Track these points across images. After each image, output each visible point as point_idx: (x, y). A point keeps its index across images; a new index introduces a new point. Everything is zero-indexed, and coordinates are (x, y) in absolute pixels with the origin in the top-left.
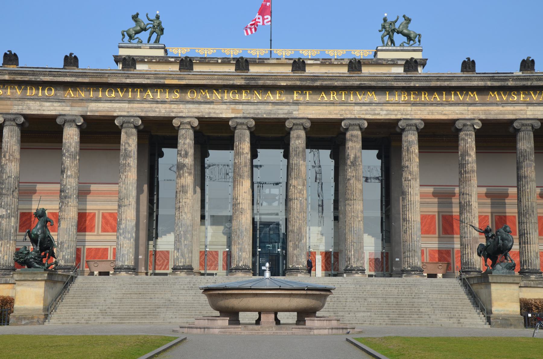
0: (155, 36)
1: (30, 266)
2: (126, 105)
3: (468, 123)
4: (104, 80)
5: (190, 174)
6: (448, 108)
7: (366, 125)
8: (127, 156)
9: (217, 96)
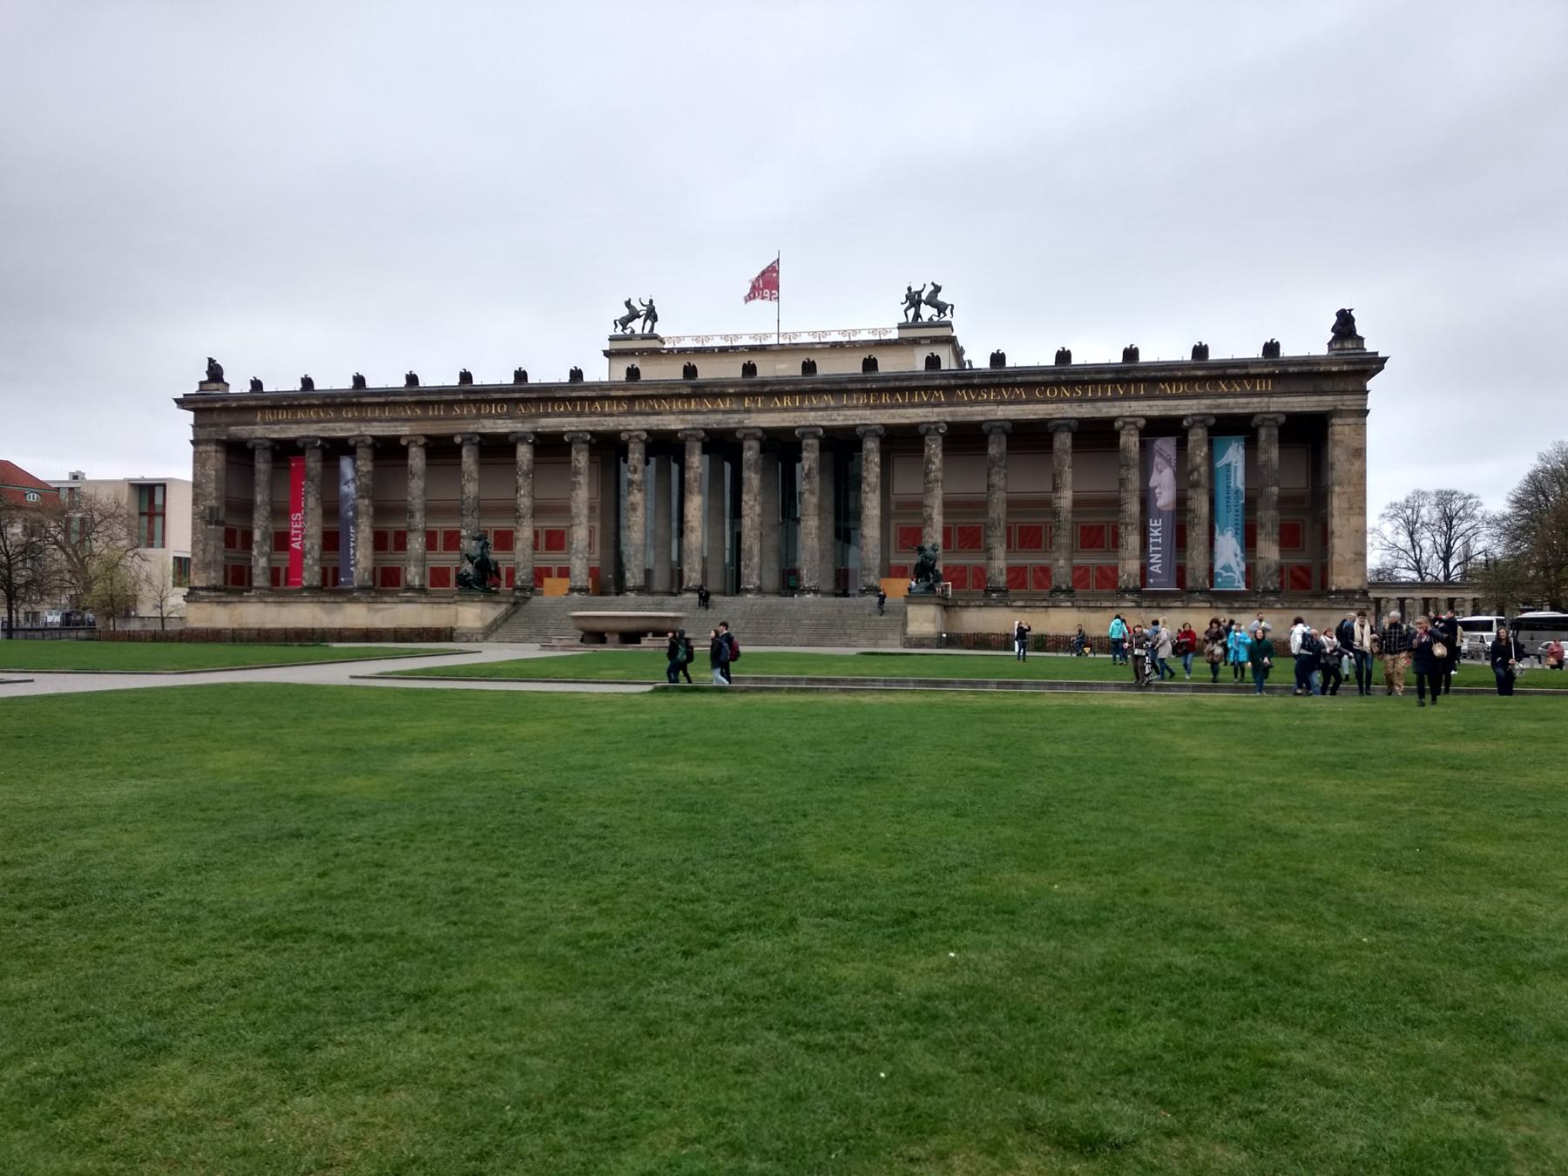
0: (649, 323)
1: (471, 588)
2: (574, 420)
3: (931, 428)
4: (550, 395)
5: (640, 490)
6: (911, 411)
7: (821, 432)
8: (577, 473)
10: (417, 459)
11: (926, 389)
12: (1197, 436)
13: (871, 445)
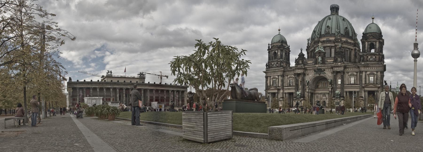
9: (128, 85)
10: (98, 90)
11: (154, 86)
12: (175, 92)
13: (149, 91)
